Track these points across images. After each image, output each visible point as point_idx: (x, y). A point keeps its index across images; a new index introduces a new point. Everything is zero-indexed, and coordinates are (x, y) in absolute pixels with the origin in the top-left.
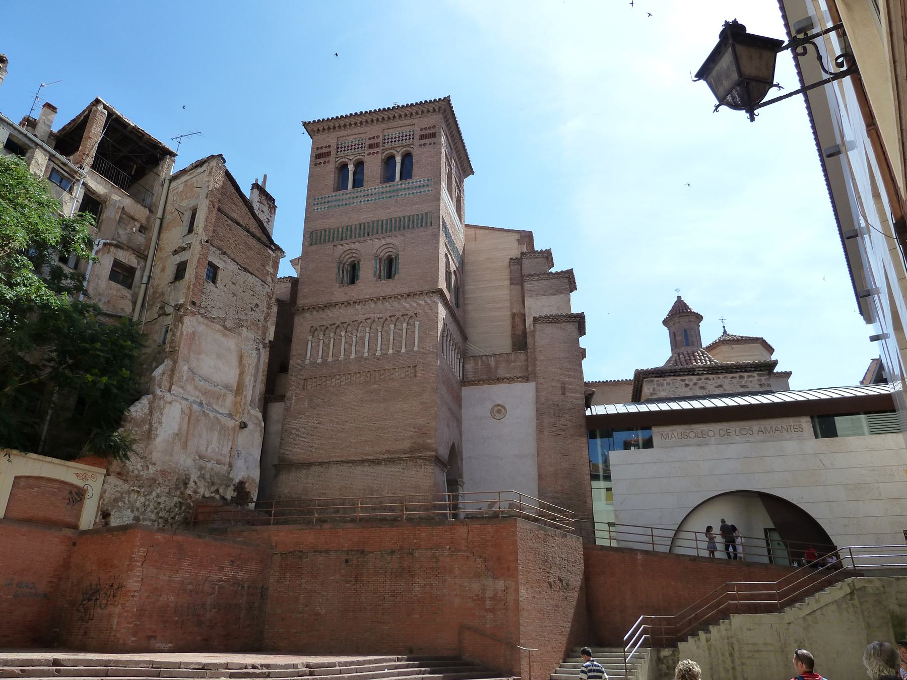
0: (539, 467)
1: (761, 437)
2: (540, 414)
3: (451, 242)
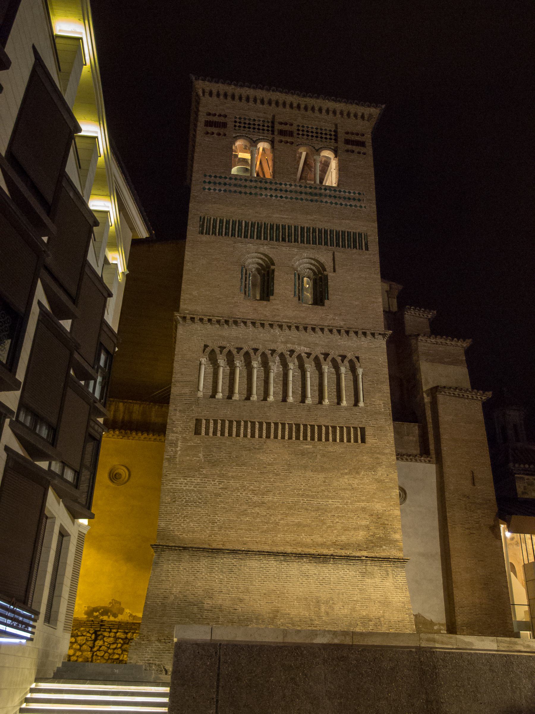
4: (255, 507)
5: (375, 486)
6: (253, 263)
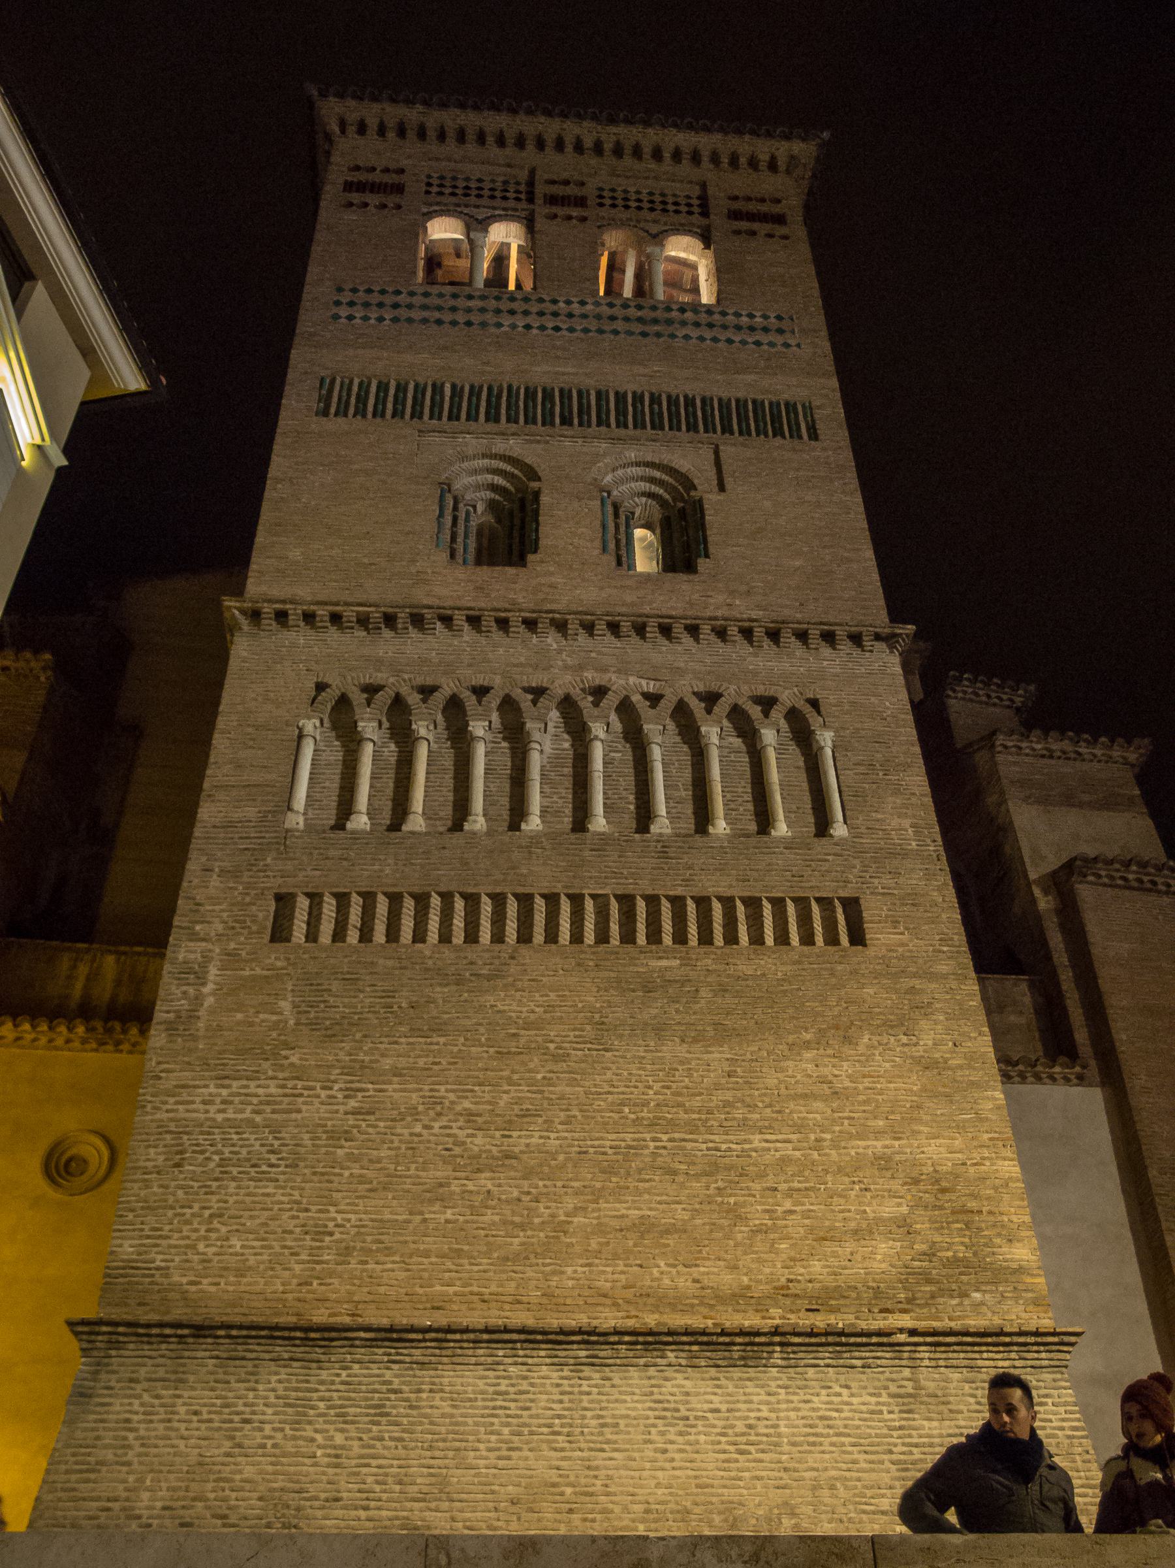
4: (479, 1171)
5: (915, 1082)
6: (478, 487)
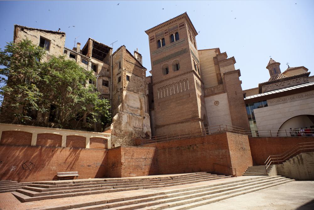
0: (231, 117)
1: (307, 97)
2: (229, 102)
3: (194, 56)
5: (193, 105)
